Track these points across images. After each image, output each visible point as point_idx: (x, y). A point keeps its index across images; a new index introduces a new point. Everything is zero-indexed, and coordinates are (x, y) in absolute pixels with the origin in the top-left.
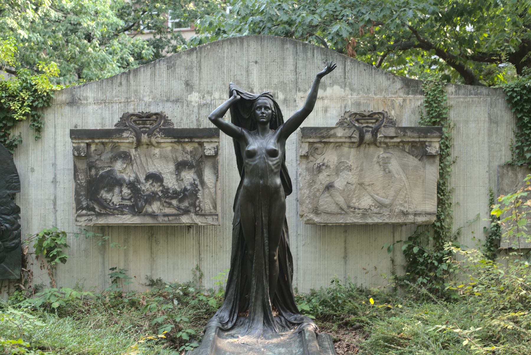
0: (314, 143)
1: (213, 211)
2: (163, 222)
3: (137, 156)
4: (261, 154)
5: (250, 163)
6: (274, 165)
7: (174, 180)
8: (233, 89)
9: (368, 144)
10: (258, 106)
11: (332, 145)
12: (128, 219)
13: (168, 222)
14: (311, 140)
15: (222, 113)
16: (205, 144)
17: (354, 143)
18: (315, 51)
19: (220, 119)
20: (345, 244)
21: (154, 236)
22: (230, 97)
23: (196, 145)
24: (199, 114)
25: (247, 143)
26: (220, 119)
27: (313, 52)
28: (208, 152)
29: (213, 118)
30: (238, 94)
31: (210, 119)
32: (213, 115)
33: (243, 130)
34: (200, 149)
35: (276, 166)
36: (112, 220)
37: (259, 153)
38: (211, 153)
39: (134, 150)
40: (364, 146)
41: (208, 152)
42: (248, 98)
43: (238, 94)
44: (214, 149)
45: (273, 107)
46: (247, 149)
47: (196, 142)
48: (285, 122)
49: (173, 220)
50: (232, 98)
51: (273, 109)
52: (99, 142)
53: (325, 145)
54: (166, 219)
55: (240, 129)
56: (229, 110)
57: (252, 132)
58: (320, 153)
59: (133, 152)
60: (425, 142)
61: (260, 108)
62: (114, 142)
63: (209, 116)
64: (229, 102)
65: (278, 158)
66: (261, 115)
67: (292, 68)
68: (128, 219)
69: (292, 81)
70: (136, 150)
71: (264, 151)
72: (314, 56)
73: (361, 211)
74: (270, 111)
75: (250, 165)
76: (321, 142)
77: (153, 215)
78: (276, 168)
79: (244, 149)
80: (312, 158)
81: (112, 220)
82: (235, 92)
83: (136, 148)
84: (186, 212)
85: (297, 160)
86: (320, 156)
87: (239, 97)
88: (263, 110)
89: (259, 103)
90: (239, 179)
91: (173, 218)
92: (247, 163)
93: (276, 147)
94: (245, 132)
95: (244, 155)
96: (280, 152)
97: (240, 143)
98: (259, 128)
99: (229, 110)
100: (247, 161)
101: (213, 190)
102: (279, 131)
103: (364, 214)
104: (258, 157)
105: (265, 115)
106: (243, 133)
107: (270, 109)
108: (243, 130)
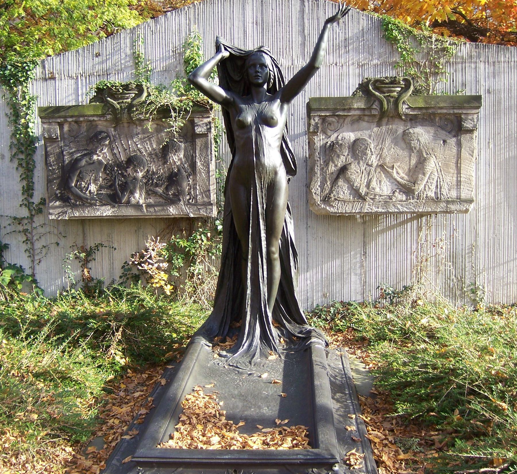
0: (326, 116)
1: (206, 199)
2: (148, 214)
3: (117, 136)
7: (160, 163)
9: (392, 117)
11: (349, 119)
12: (107, 211)
13: (154, 214)
17: (374, 115)
20: (364, 237)
21: (141, 230)
28: (199, 130)
36: (87, 213)
39: (113, 129)
40: (387, 120)
41: (199, 130)
44: (207, 125)
49: (160, 211)
52: (72, 121)
54: (152, 210)
58: (333, 128)
59: (112, 131)
60: (461, 114)
62: (90, 121)
66: (254, 75)
68: (107, 211)
70: (115, 130)
73: (383, 197)
76: (333, 116)
77: (138, 206)
81: (87, 213)
83: (115, 128)
84: (174, 200)
86: (332, 132)
90: (230, 156)
91: (160, 208)
95: (235, 127)
103: (386, 202)
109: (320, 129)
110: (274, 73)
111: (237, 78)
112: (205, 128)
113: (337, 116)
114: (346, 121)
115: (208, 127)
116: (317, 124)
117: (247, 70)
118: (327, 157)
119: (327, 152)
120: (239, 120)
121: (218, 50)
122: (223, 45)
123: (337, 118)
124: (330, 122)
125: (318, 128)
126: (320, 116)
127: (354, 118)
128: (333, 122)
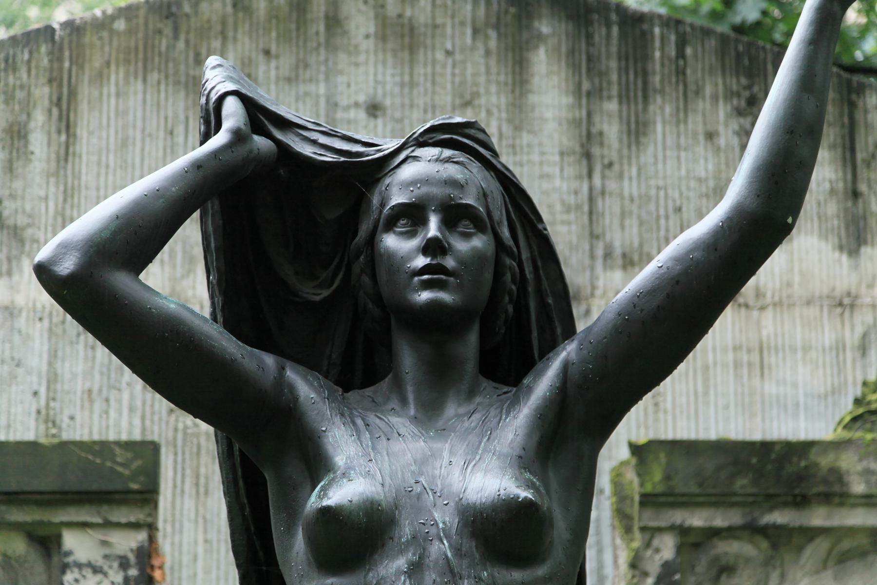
0: (713, 533)
4: (420, 541)
10: (397, 198)
15: (138, 238)
16: (71, 540)
19: (121, 280)
23: (18, 546)
24: (53, 379)
25: (316, 465)
26: (121, 280)
29: (66, 267)
31: (43, 272)
32: (64, 248)
33: (291, 374)
34: (39, 567)
37: (406, 530)
42: (329, 158)
44: (124, 564)
45: (499, 214)
46: (314, 502)
47: (17, 527)
50: (219, 139)
51: (505, 233)
53: (775, 546)
55: (269, 360)
56: (191, 232)
57: (353, 395)
61: (412, 215)
63: (43, 254)
64: (198, 165)
66: (421, 261)
69: (568, 209)
71: (444, 517)
74: (478, 242)
76: (753, 530)
79: (292, 510)
82: (232, 109)
88: (433, 228)
93: (530, 485)
94: (305, 388)
95: (295, 550)
96: (561, 529)
97: (266, 459)
98: (408, 359)
99: (191, 232)
102: (544, 384)
104: (401, 563)
105: (450, 262)
106: (292, 388)
108: (291, 374)
113: (765, 531)
114: (808, 551)
117: (372, 240)
123: (764, 544)
126: (683, 531)
127: (846, 544)
128: (748, 560)
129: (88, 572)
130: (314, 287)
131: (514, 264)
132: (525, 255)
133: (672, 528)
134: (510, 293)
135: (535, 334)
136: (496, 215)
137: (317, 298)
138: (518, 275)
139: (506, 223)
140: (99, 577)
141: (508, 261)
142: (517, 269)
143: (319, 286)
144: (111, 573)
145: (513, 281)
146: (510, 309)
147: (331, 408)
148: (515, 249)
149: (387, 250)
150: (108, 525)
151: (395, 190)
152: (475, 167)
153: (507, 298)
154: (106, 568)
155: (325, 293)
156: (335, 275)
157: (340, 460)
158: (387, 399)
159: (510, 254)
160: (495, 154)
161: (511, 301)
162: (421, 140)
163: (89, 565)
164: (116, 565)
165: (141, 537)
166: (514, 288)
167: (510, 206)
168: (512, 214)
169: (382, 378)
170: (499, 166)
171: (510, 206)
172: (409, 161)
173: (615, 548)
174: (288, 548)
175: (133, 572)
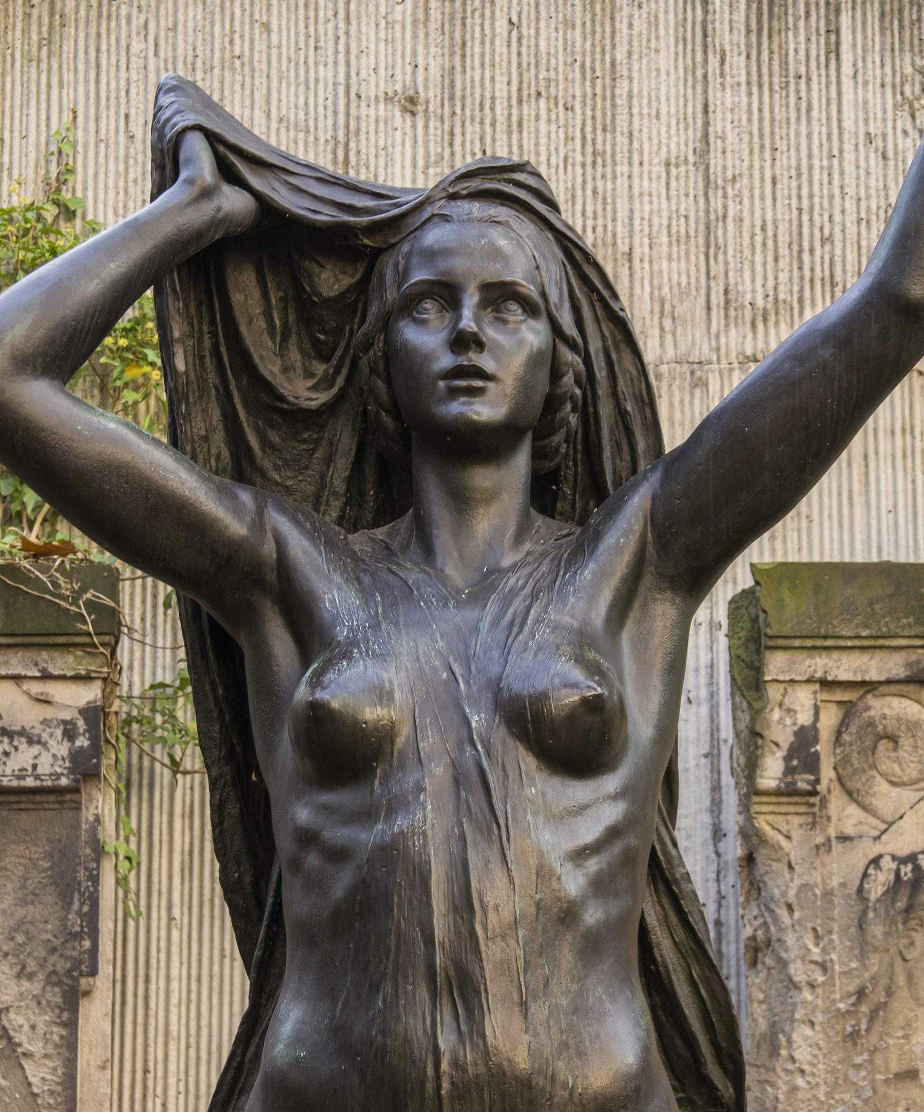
5: (336, 834)
6: (580, 855)
8: (181, 121)
10: (419, 275)
14: (845, 667)
18: (845, 20)
22: (159, 189)
27: (833, 31)
30: (228, 174)
35: (593, 865)
38: (44, 768)
42: (326, 216)
43: (228, 174)
44: (70, 733)
48: (674, 436)
58: (912, 771)
65: (611, 782)
66: (446, 361)
67: (681, 142)
72: (835, 51)
75: (338, 855)
78: (600, 886)
80: (853, 810)
85: (718, 834)
86: (908, 795)
87: (234, 202)
89: (431, 255)
90: (230, 989)
92: (307, 838)
95: (282, 757)
100: (303, 815)
101: (41, 1074)
107: (530, 308)
109: (827, 773)
110: (587, 361)
111: (302, 390)
112: (63, 749)
115: (82, 742)
116: (805, 739)
118: (875, 962)
119: (877, 930)
120: (317, 713)
121: (167, 163)
122: (212, 138)
124: (891, 725)
125: (812, 764)
129: (22, 743)
130: (309, 389)
131: (578, 359)
132: (595, 345)
133: (810, 681)
134: (572, 398)
135: (607, 454)
136: (553, 296)
137: (313, 405)
138: (584, 373)
139: (567, 305)
140: (36, 749)
141: (568, 356)
142: (582, 367)
143: (315, 388)
144: (52, 743)
145: (578, 382)
146: (573, 420)
147: (329, 561)
148: (579, 340)
149: (405, 344)
150: (46, 676)
151: (414, 260)
152: (526, 228)
153: (569, 406)
154: (45, 737)
155: (322, 398)
156: (337, 372)
157: (342, 633)
158: (405, 548)
159: (572, 345)
160: (554, 207)
161: (574, 410)
162: (451, 190)
163: (22, 733)
164: (59, 732)
165: (90, 693)
166: (578, 391)
167: (573, 280)
168: (577, 291)
169: (403, 512)
170: (559, 225)
171: (573, 280)
172: (435, 220)
173: (734, 709)
174: (271, 749)
175: (82, 742)
